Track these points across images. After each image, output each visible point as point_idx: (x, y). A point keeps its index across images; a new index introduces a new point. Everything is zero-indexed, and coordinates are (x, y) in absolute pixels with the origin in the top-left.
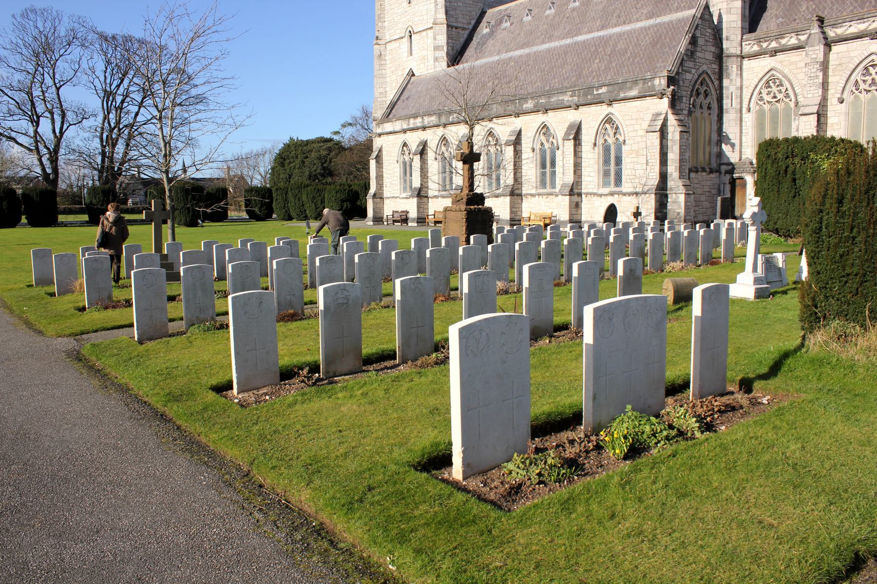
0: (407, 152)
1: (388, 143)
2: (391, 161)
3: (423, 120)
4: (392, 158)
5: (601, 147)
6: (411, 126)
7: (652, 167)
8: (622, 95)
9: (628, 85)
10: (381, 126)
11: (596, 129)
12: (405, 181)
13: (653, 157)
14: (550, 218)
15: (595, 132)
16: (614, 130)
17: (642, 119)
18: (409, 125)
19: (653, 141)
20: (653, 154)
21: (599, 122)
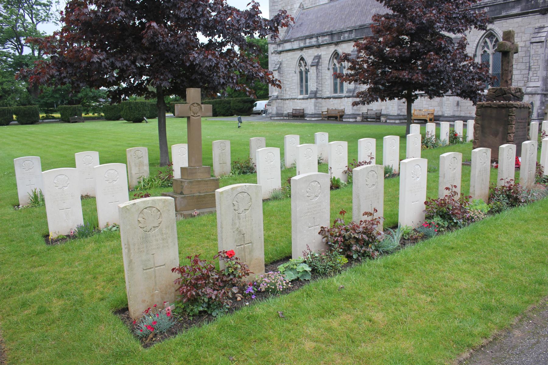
0: (303, 65)
1: (288, 58)
2: (290, 72)
3: (318, 39)
4: (291, 69)
5: (480, 57)
6: (307, 44)
7: (535, 72)
8: (504, 14)
9: (510, 5)
10: (282, 45)
11: (476, 43)
12: (301, 86)
13: (536, 64)
14: (433, 114)
15: (475, 45)
16: (493, 43)
17: (524, 33)
18: (305, 43)
19: (537, 50)
20: (535, 61)
21: (480, 37)
